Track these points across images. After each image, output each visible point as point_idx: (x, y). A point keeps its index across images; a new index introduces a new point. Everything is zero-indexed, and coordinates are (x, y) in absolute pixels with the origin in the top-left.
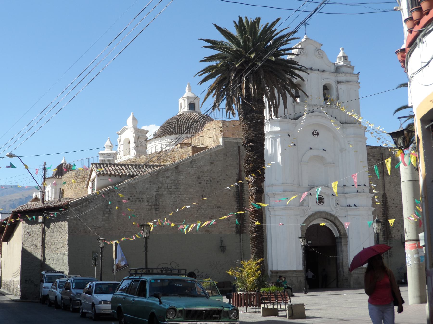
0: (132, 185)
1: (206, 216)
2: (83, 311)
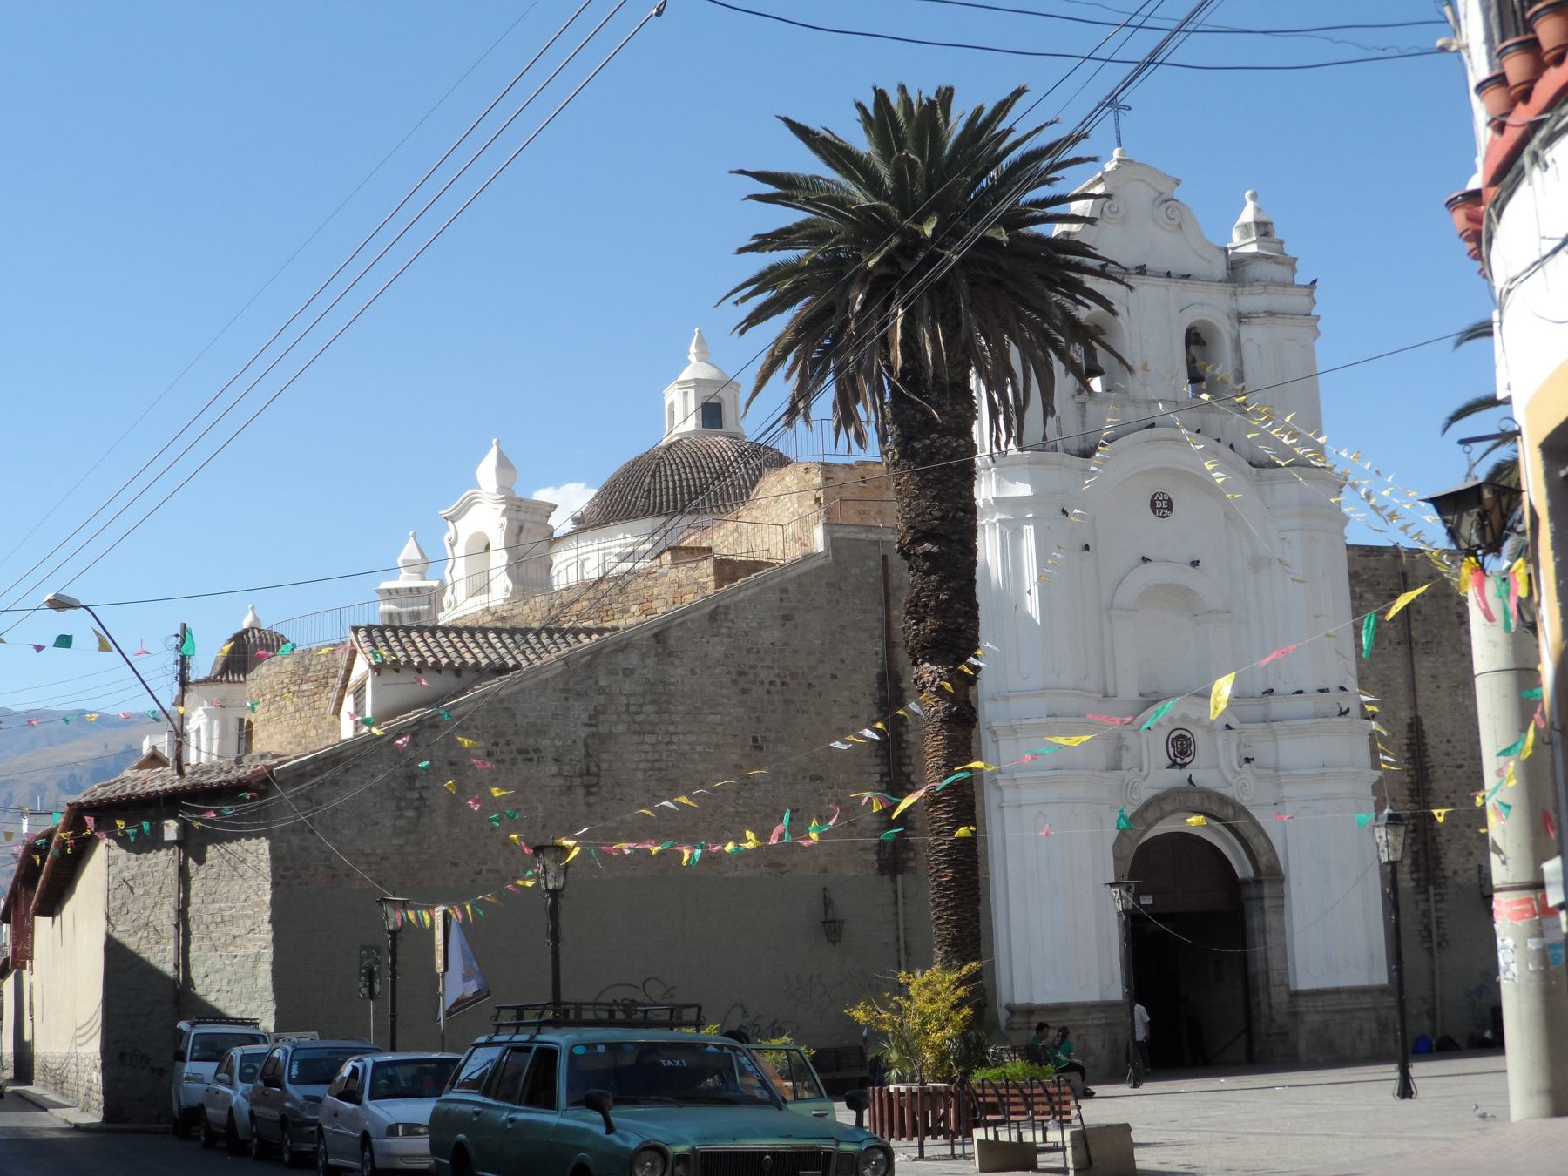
0: (501, 701)
2: (331, 1161)
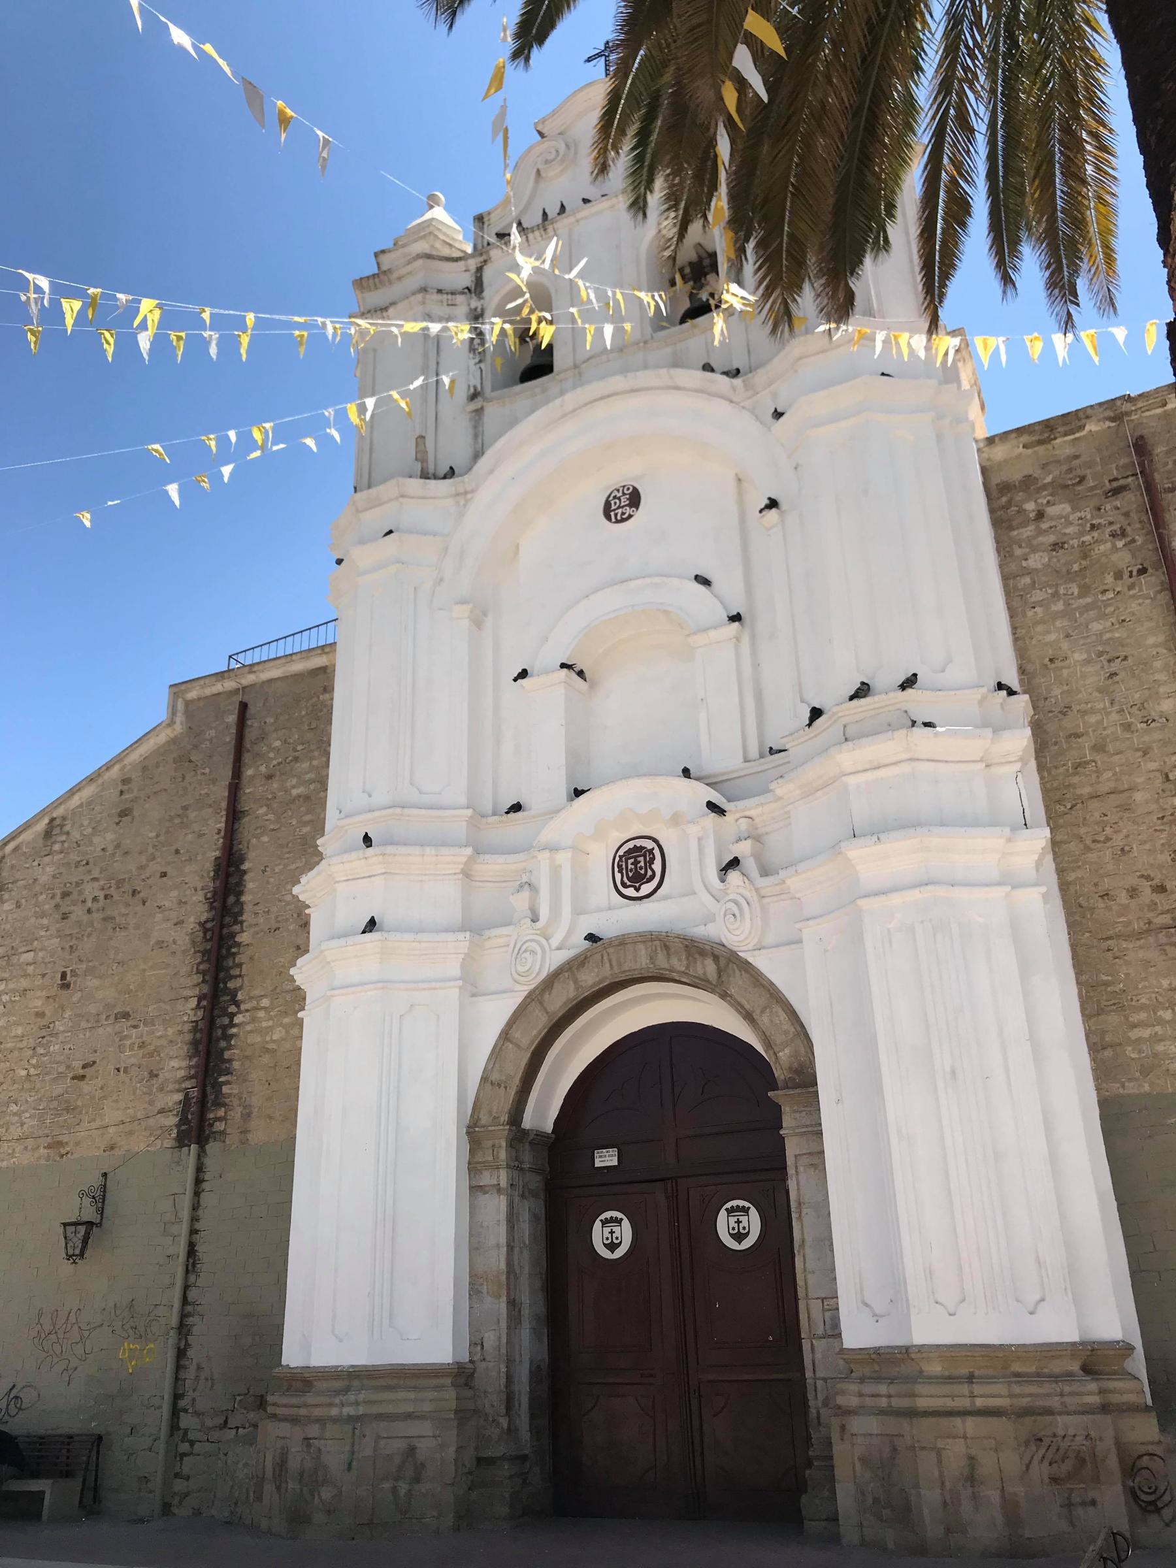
1: (62, 1069)
